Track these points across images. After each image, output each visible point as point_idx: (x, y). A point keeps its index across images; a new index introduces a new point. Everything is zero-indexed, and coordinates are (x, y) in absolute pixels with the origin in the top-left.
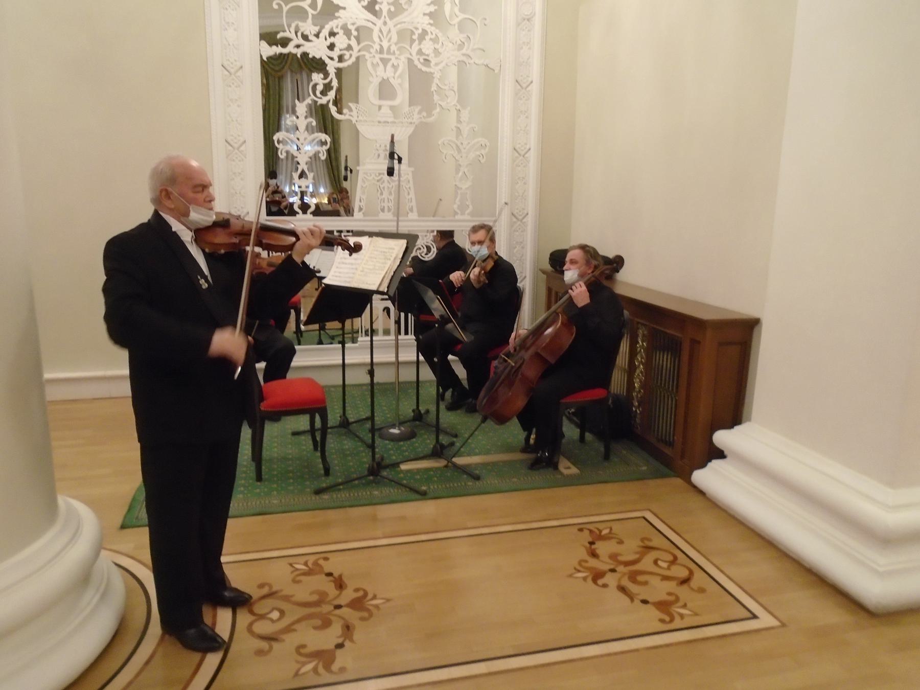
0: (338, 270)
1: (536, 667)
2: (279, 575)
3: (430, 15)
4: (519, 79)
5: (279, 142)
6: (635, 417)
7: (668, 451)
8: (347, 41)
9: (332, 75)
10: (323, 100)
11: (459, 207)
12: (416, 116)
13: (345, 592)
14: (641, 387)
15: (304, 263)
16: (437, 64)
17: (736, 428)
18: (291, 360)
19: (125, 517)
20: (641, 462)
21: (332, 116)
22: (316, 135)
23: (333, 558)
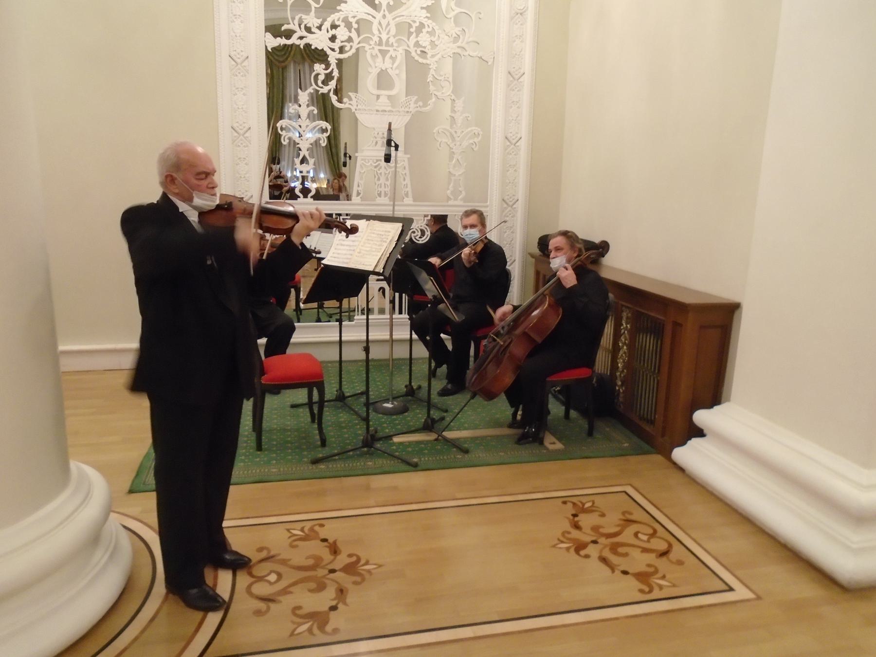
0: (337, 251)
1: (520, 632)
2: (276, 539)
3: (427, 8)
4: (512, 71)
5: (282, 129)
6: (618, 395)
7: (648, 428)
8: (348, 34)
9: (333, 65)
10: (325, 90)
12: (412, 105)
13: (339, 557)
14: (624, 367)
15: (302, 244)
16: (433, 56)
18: (290, 337)
19: (133, 482)
20: (623, 439)
21: (333, 105)
22: (317, 122)
23: (328, 524)
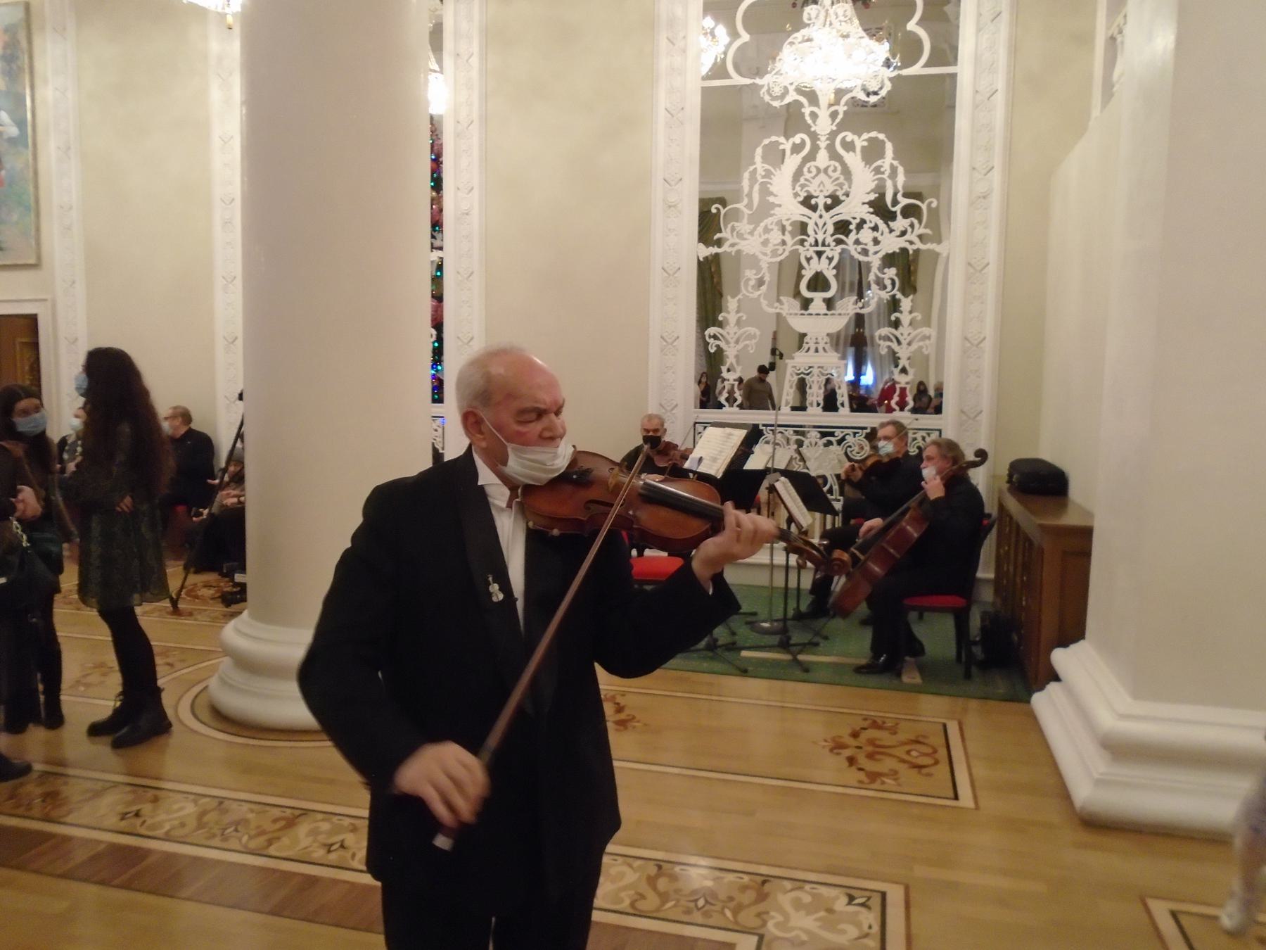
3: (871, 204)
8: (781, 237)
11: (897, 404)
16: (876, 253)
17: (1073, 647)
